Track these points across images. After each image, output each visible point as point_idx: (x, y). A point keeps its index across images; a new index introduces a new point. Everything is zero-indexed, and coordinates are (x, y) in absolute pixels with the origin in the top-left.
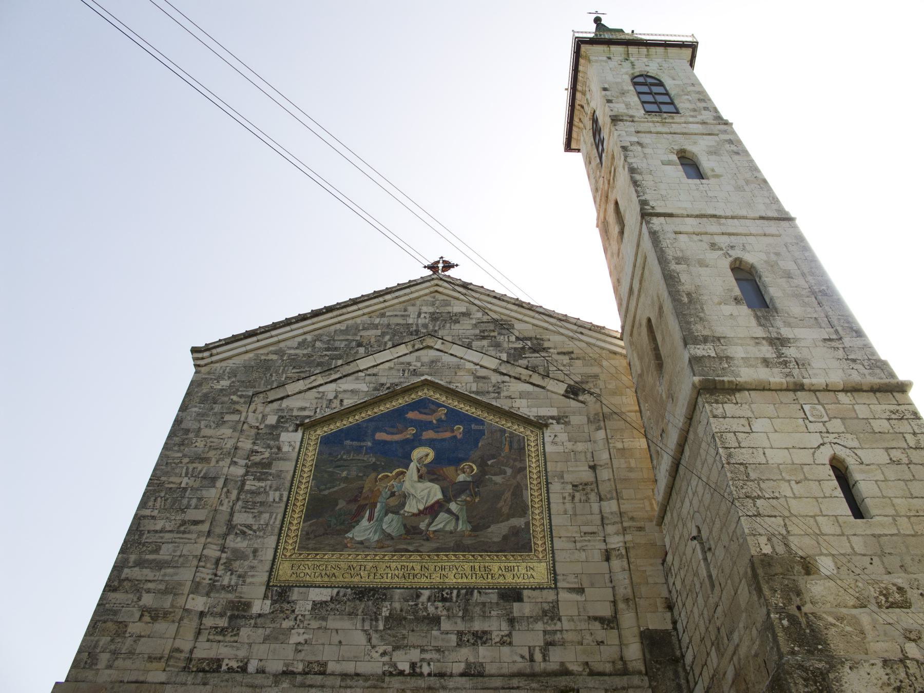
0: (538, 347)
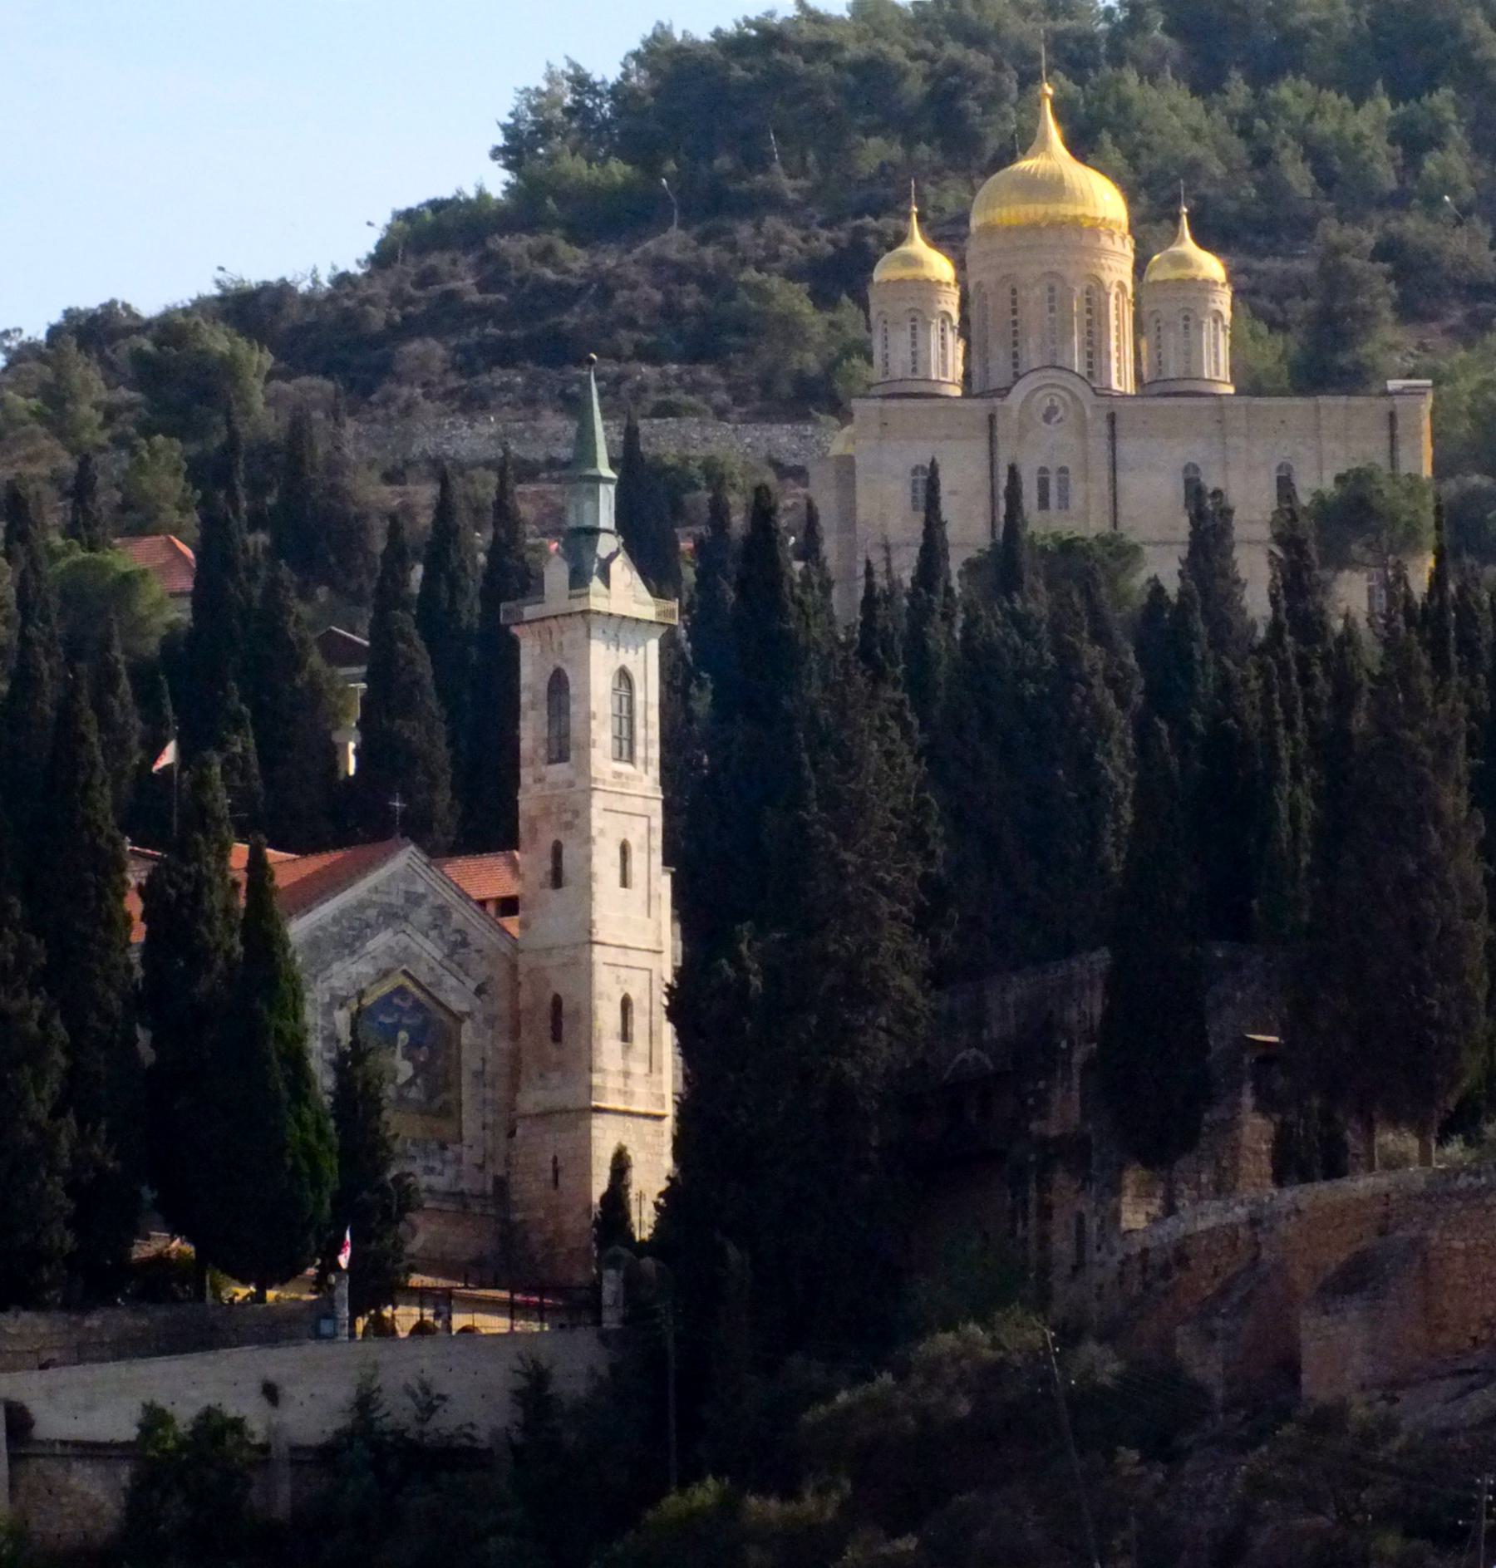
0: (464, 944)
